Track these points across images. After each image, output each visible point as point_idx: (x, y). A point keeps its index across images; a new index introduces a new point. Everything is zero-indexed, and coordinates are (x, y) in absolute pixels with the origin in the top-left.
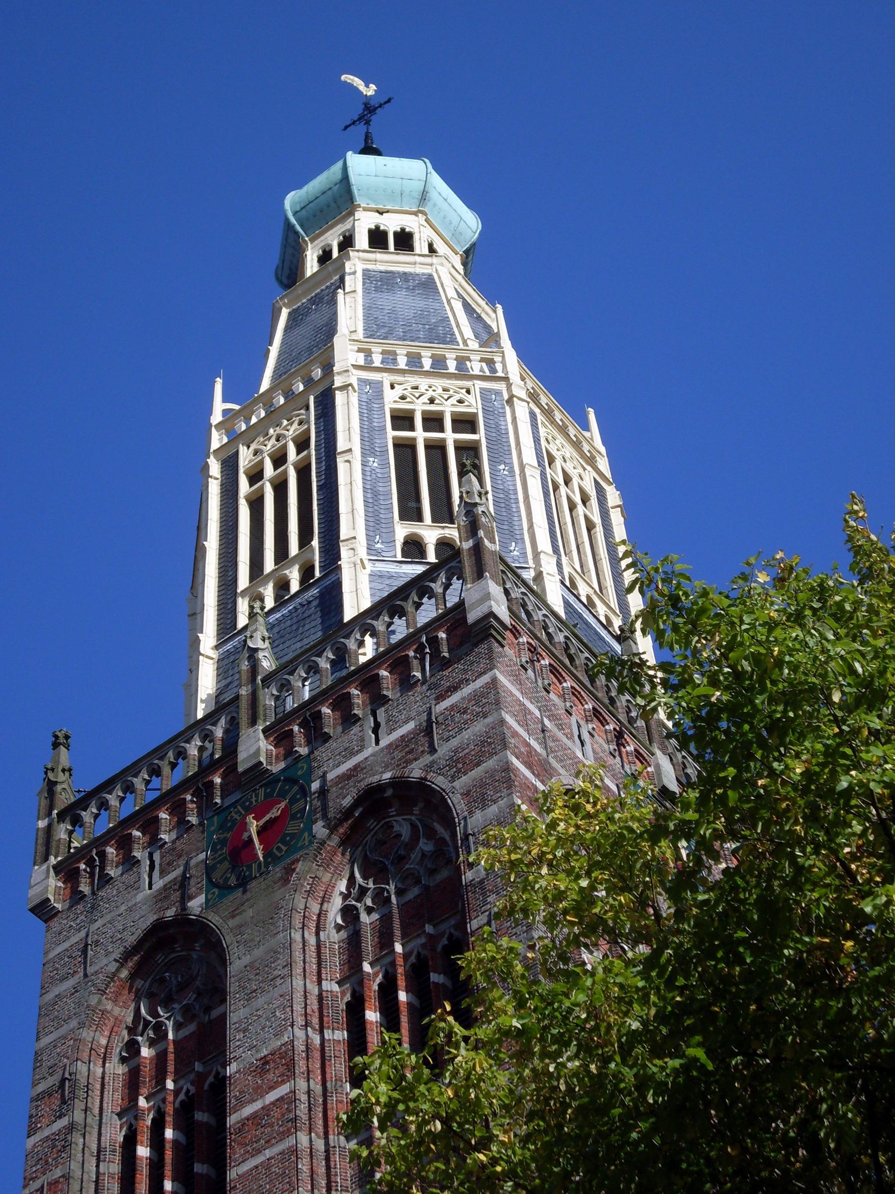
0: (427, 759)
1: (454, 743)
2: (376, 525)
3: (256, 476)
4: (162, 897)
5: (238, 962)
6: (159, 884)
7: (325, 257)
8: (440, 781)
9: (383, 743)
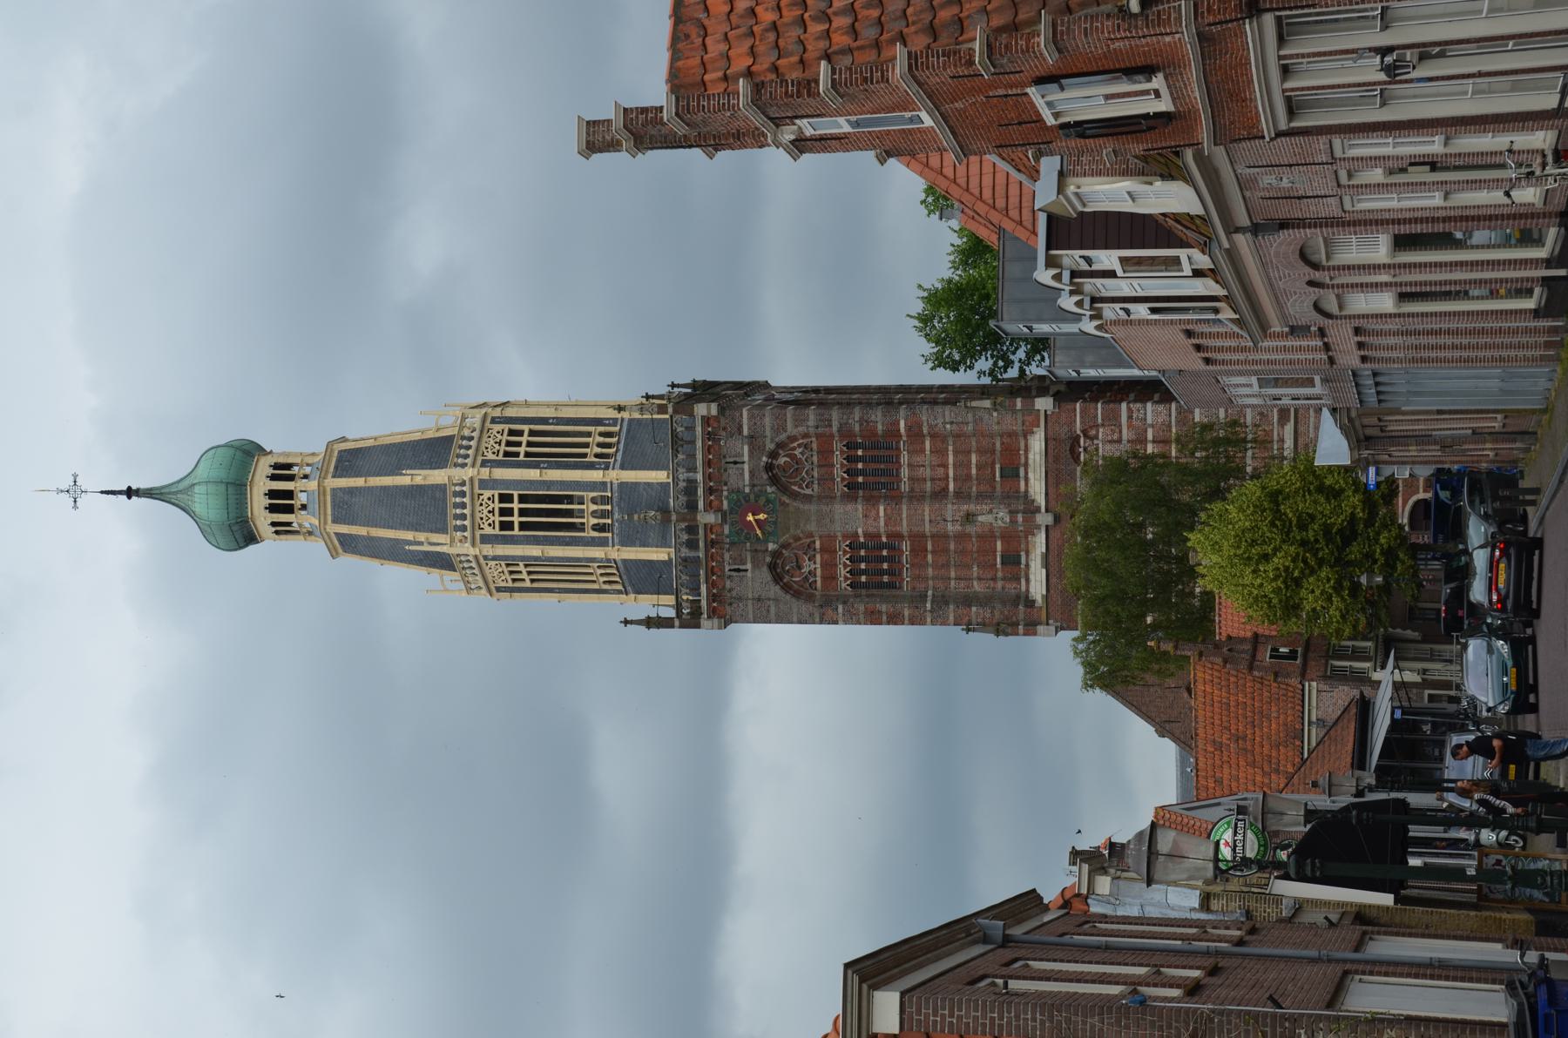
0: (768, 441)
1: (768, 429)
2: (591, 466)
3: (506, 526)
4: (756, 565)
5: (812, 527)
6: (749, 566)
7: (272, 509)
8: (783, 437)
9: (746, 458)
